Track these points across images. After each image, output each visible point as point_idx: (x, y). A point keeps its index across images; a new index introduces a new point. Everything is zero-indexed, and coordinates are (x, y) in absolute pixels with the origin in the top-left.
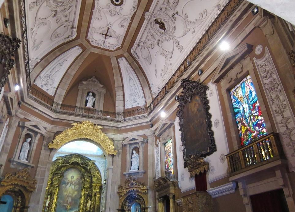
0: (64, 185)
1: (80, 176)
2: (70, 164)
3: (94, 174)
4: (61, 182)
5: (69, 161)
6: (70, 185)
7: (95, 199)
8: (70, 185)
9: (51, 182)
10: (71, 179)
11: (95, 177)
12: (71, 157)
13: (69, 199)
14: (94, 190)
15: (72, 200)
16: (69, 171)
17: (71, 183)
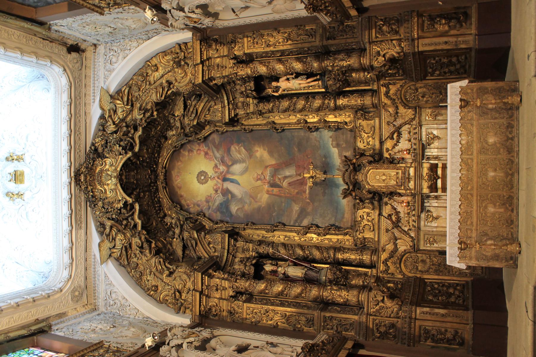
0: (234, 208)
1: (196, 147)
2: (130, 200)
3: (161, 84)
4: (222, 221)
5: (121, 205)
6: (232, 181)
7: (263, 57)
8: (232, 181)
9: (200, 274)
10: (211, 184)
11: (172, 79)
12: (100, 204)
13: (285, 177)
14: (226, 73)
15: (287, 164)
16: (182, 196)
17: (225, 180)
